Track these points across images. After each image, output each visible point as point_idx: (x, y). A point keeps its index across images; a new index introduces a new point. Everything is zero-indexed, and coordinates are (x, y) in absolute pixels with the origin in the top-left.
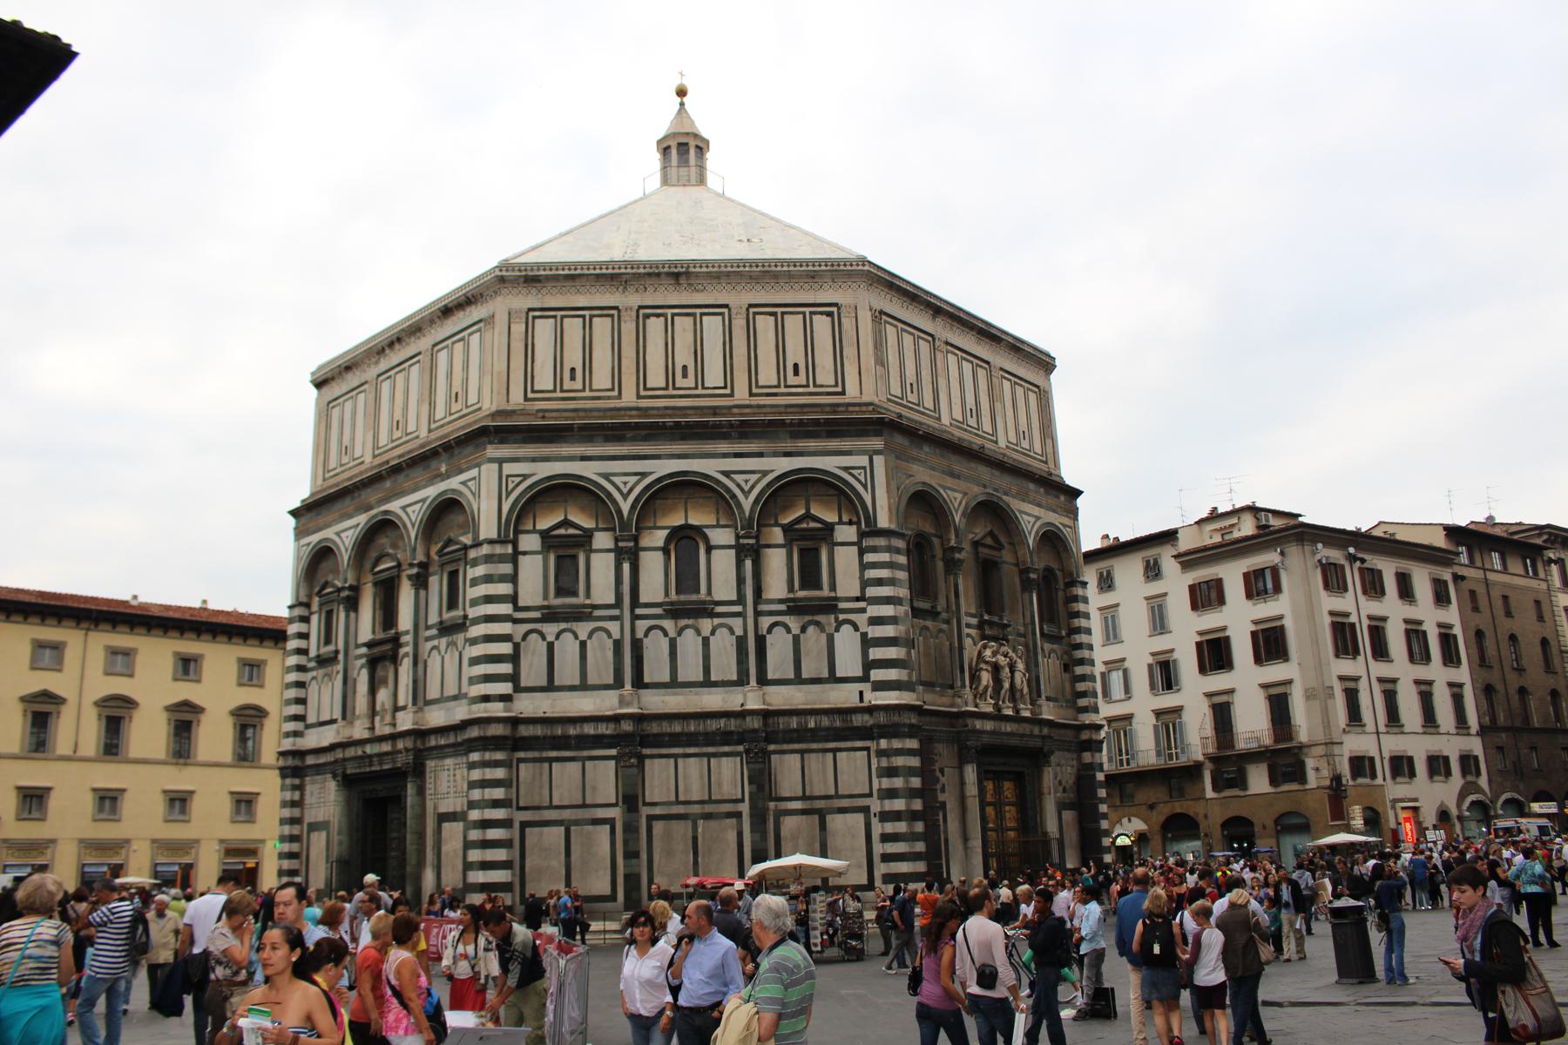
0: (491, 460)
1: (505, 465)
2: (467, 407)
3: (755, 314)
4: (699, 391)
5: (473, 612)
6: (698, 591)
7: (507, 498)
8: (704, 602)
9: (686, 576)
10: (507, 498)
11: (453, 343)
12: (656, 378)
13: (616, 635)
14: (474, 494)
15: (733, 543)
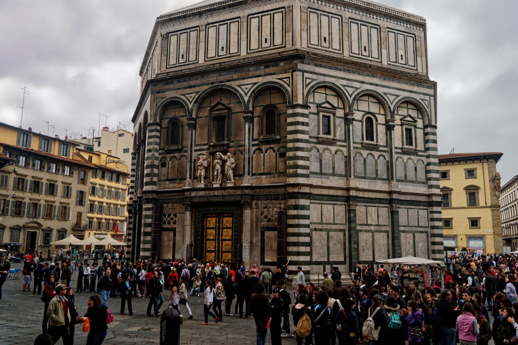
0: (300, 71)
1: (305, 74)
2: (274, 46)
3: (388, 31)
4: (370, 58)
5: (289, 137)
6: (373, 140)
7: (306, 88)
8: (376, 145)
9: (370, 134)
10: (306, 88)
11: (262, 16)
12: (355, 50)
13: (345, 154)
14: (289, 85)
15: (384, 123)
